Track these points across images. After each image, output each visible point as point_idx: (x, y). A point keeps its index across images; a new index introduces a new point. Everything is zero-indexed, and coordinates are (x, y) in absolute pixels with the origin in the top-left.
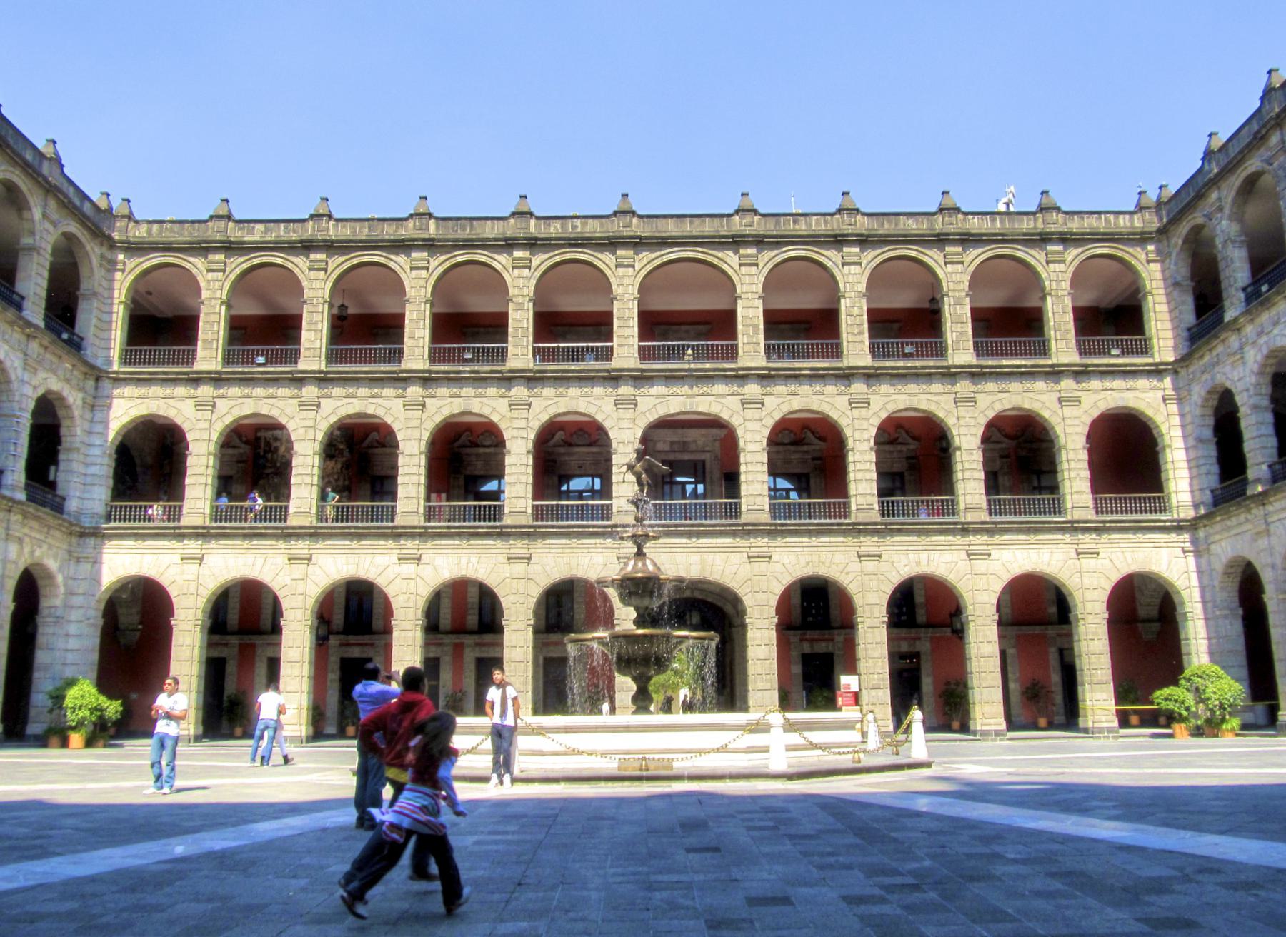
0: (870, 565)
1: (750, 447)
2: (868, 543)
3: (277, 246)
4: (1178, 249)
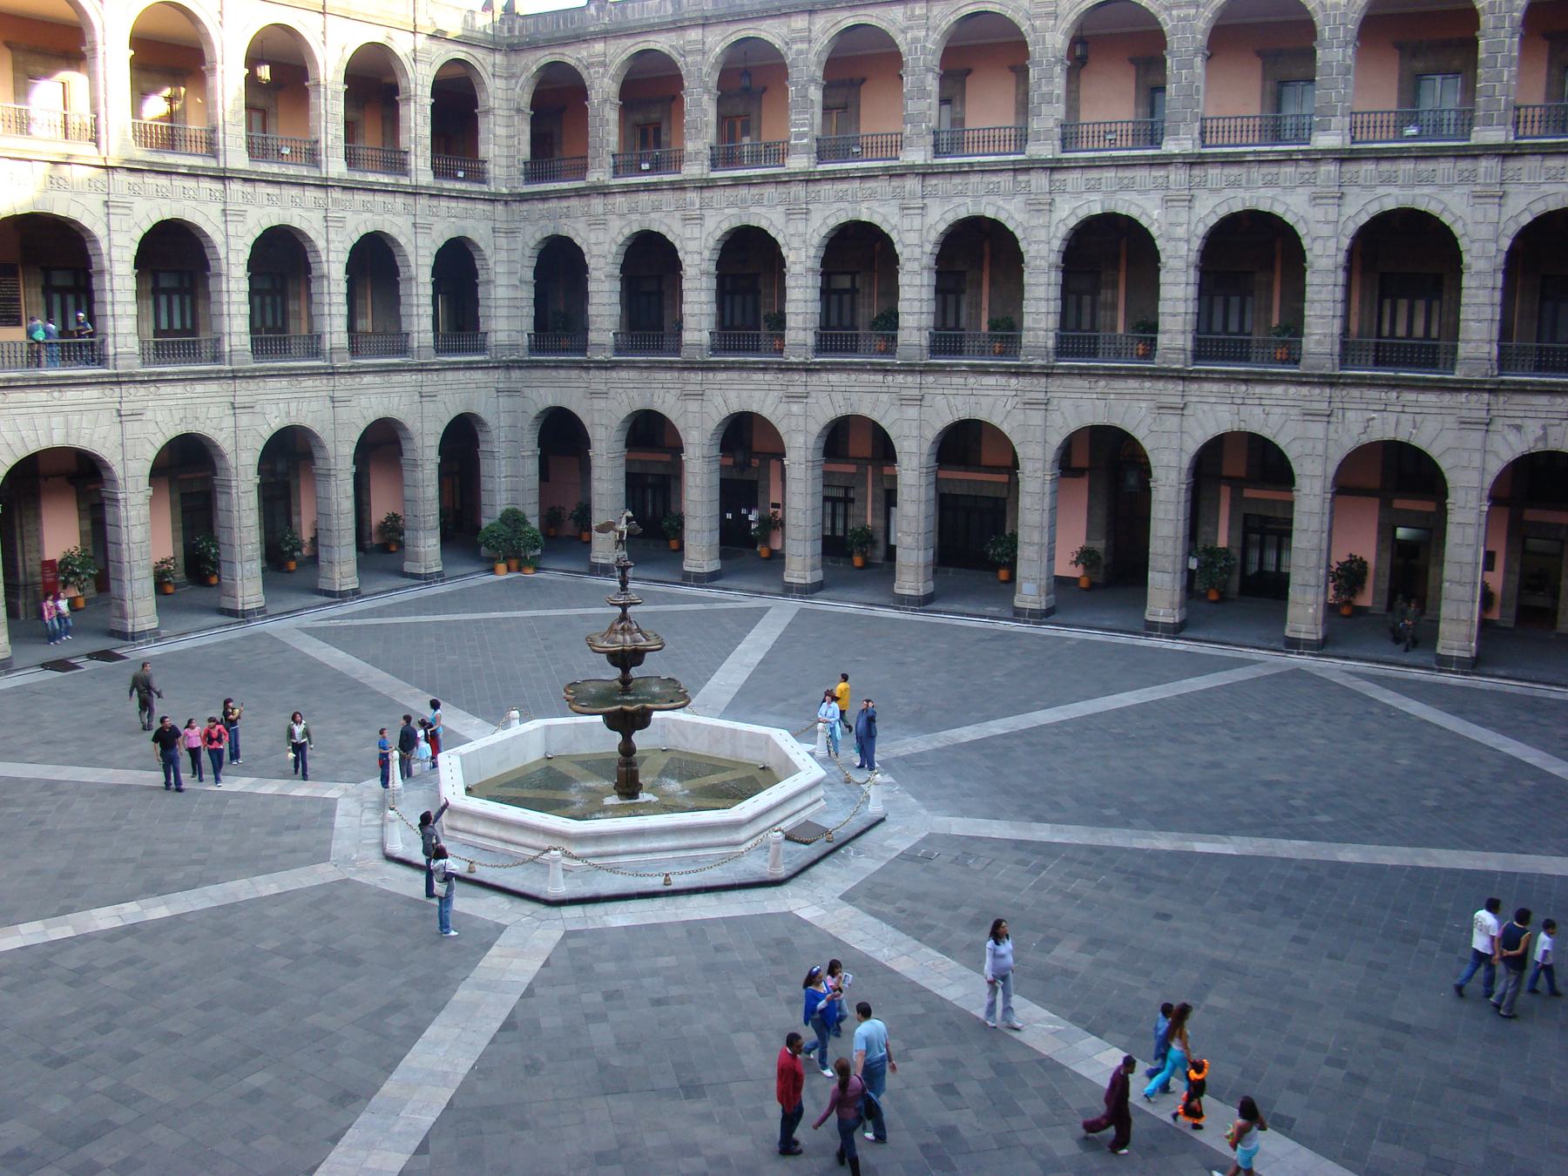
0: (244, 420)
4: (529, 74)
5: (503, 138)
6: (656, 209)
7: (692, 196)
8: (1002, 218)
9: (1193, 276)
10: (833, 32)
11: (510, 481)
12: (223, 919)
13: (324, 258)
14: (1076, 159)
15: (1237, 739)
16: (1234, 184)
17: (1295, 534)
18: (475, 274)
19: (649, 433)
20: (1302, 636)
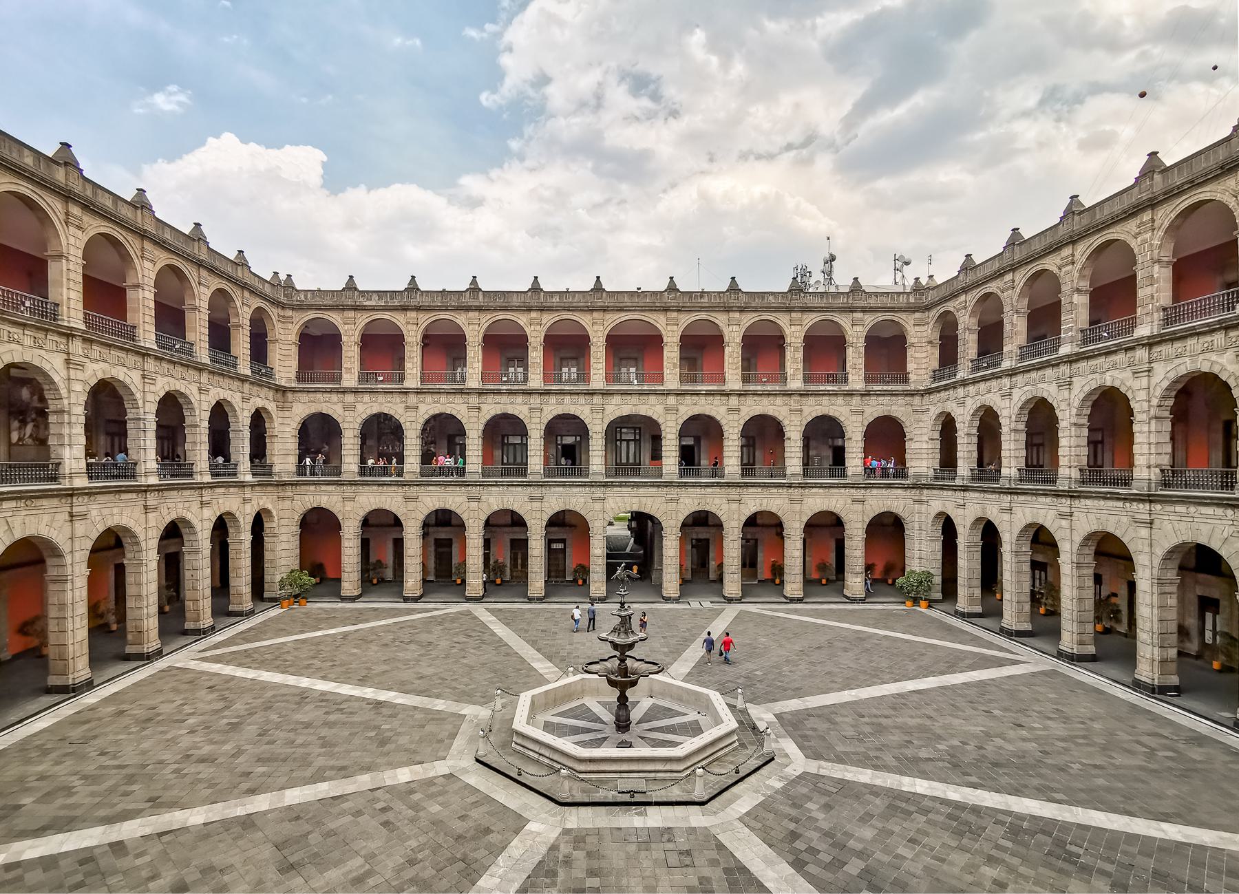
0: (734, 506)
1: (669, 436)
2: (734, 493)
3: (386, 308)
5: (921, 361)
6: (989, 391)
8: (1216, 370)
10: (1089, 252)
11: (922, 554)
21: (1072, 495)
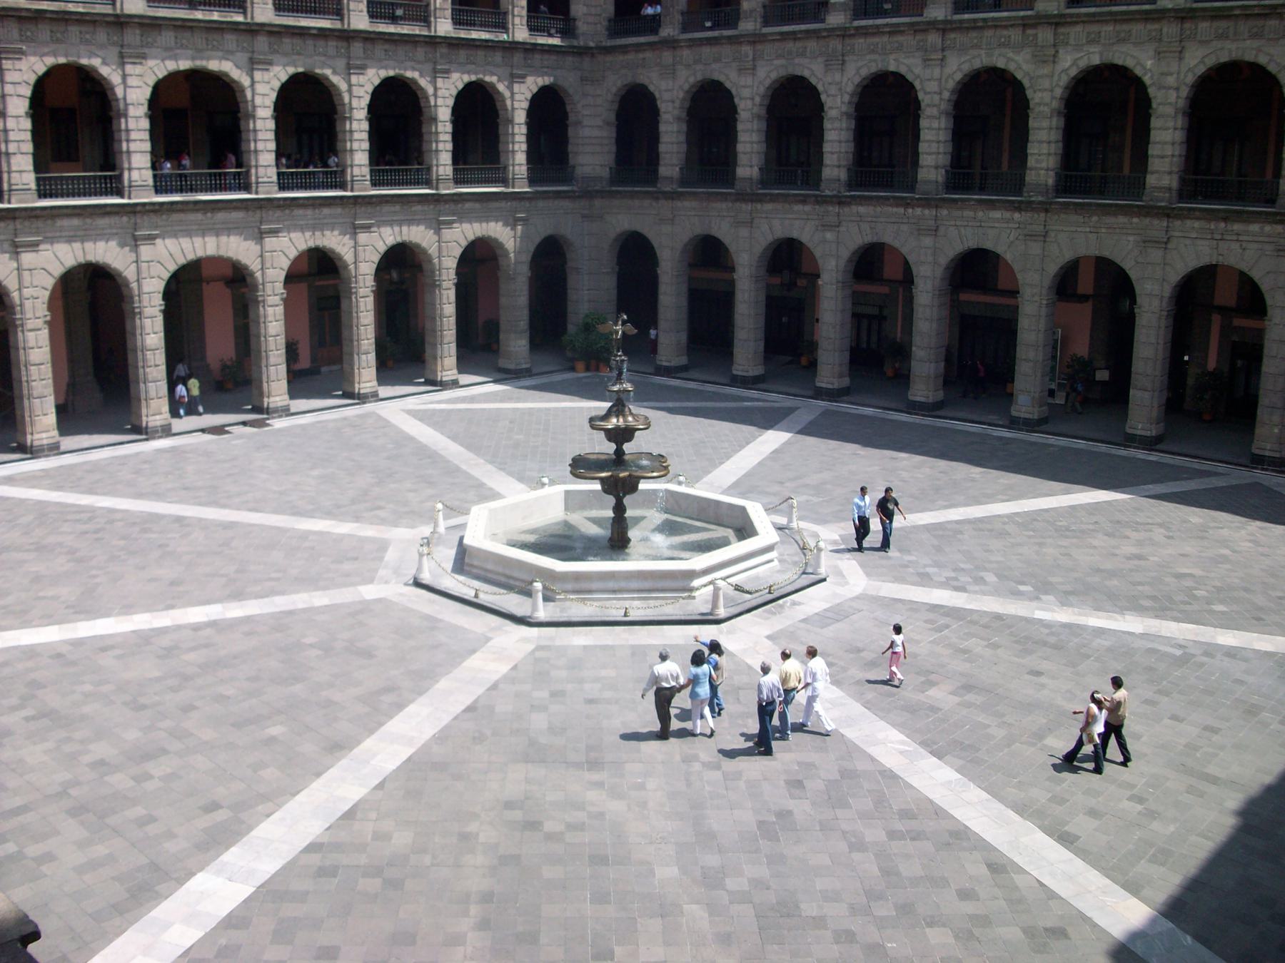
6: (717, 60)
7: (747, 49)
8: (1012, 67)
9: (1180, 121)
12: (281, 621)
13: (432, 103)
14: (1078, 15)
15: (1169, 537)
16: (1223, 36)
17: (1265, 360)
18: (565, 115)
19: (709, 253)
20: (1267, 454)
21: (840, 201)
